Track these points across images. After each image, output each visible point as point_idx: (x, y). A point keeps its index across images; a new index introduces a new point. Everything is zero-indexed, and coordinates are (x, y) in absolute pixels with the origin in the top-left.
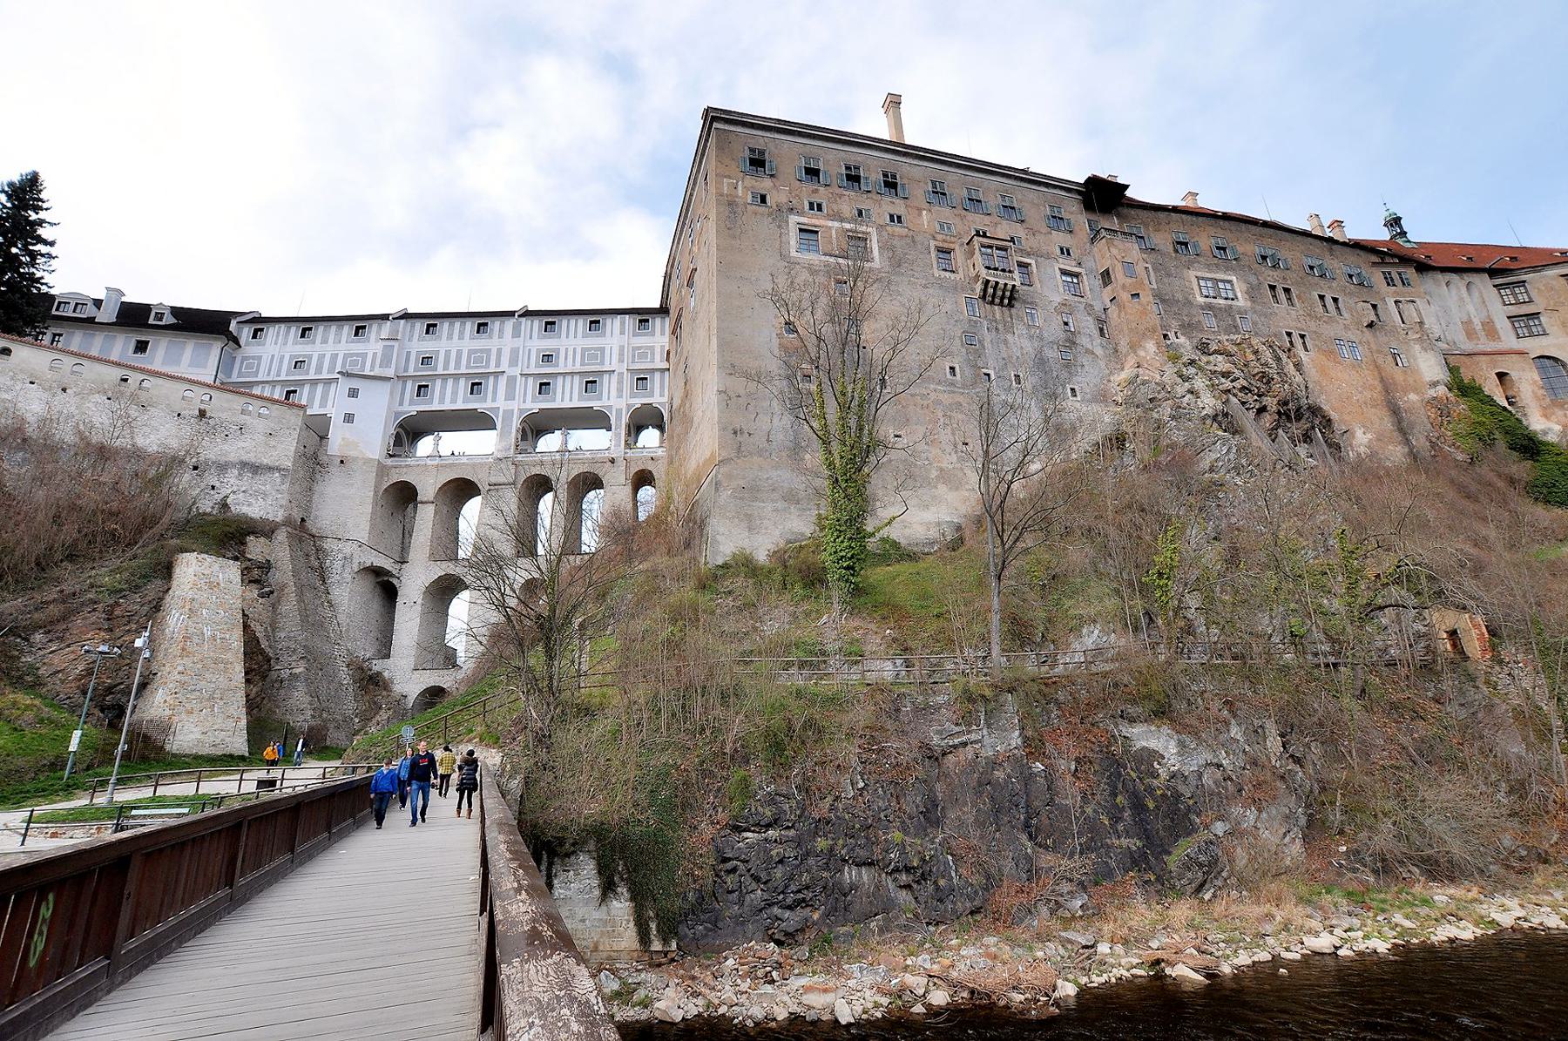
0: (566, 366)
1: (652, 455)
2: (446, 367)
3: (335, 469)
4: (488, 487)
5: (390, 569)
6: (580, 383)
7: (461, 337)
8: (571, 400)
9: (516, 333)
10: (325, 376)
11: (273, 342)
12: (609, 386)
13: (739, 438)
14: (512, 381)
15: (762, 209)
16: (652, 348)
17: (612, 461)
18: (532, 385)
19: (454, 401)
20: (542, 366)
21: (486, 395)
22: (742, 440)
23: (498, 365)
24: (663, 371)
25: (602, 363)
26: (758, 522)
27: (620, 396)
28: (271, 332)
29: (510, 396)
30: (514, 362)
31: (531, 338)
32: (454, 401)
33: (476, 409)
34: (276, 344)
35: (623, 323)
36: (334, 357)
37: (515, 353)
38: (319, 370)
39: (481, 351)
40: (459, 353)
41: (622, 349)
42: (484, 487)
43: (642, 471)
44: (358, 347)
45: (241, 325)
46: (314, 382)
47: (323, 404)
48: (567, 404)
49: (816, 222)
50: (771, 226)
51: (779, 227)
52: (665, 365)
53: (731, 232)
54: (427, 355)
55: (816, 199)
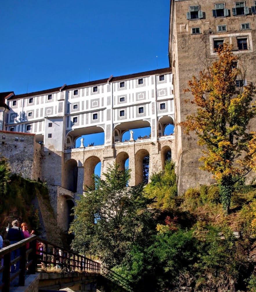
0: (130, 102)
1: (169, 139)
2: (83, 109)
3: (47, 157)
4: (103, 159)
5: (70, 195)
6: (137, 109)
7: (87, 95)
8: (133, 117)
9: (108, 91)
10: (40, 118)
11: (20, 106)
12: (148, 108)
13: (191, 141)
14: (108, 111)
15: (198, 36)
16: (166, 89)
17: (153, 144)
18: (117, 112)
19: (87, 123)
20: (120, 103)
21: (99, 119)
22: (191, 142)
23: (103, 105)
24: (172, 99)
25: (145, 99)
26: (199, 176)
27: (153, 113)
28: (19, 102)
29: (108, 119)
30: (108, 104)
31: (115, 91)
32: (87, 123)
33: (96, 126)
34: (21, 107)
35: (152, 79)
36: (42, 109)
37: (108, 98)
38: (37, 116)
39: (96, 100)
40: (87, 102)
41: (153, 91)
42: (102, 159)
43: (166, 146)
44: (50, 104)
45: (9, 101)
46: (36, 122)
47: (40, 130)
48: (132, 120)
49: (221, 36)
50: (202, 43)
51: (205, 42)
52: (172, 96)
53: (184, 49)
54: (75, 104)
55: (223, 24)
